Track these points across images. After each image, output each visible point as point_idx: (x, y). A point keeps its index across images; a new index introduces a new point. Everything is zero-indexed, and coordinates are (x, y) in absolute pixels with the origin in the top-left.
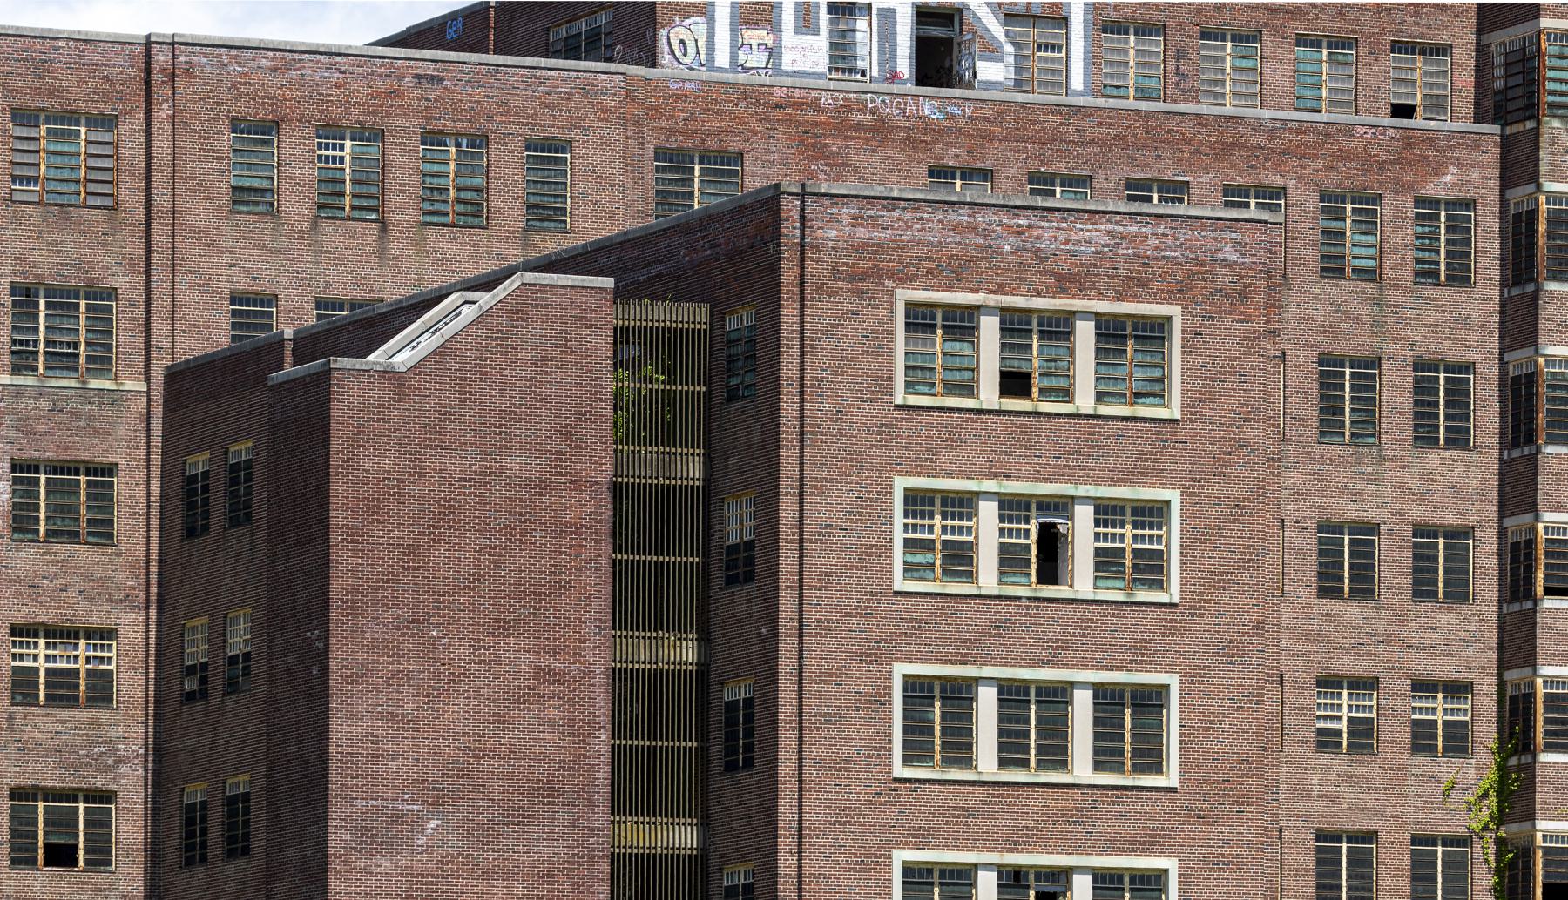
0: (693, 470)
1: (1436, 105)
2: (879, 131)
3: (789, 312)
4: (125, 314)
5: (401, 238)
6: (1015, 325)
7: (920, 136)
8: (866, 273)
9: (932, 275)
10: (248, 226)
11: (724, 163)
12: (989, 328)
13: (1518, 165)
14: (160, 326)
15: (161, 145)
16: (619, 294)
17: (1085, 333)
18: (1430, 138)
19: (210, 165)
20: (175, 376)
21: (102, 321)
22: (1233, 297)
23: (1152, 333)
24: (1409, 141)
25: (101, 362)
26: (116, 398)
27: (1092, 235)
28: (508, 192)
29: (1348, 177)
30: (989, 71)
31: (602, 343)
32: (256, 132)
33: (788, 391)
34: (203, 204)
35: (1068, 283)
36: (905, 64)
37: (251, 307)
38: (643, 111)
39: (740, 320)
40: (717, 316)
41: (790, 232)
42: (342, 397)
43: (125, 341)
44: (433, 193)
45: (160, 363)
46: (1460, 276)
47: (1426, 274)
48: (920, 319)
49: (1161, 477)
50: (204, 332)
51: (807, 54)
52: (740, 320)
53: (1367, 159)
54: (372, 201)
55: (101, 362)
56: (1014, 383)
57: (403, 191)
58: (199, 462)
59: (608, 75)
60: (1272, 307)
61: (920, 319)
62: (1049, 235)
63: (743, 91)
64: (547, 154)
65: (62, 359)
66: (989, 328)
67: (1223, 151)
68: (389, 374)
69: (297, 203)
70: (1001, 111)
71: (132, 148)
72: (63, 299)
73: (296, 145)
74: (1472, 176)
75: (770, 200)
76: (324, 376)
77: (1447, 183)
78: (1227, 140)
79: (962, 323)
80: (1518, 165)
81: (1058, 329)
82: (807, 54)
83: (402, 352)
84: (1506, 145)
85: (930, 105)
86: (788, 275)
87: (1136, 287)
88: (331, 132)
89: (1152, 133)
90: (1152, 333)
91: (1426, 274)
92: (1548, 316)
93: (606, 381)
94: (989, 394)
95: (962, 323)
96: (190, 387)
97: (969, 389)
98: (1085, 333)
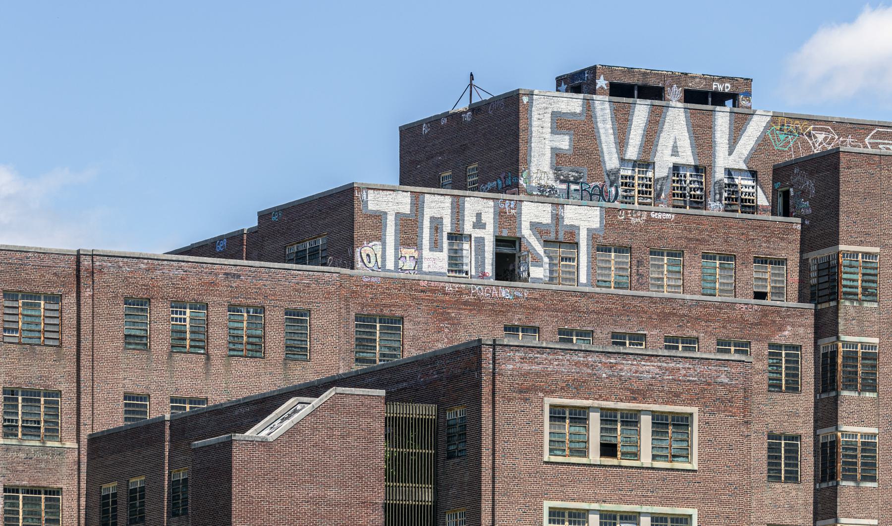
0: (427, 496)
1: (778, 292)
2: (477, 305)
3: (486, 410)
4: (66, 406)
5: (217, 363)
6: (609, 418)
7: (499, 308)
8: (528, 389)
9: (564, 390)
10: (134, 357)
11: (393, 324)
12: (595, 419)
13: (826, 326)
14: (86, 413)
15: (86, 311)
16: (388, 399)
17: (646, 422)
18: (777, 311)
19: (111, 324)
20: (94, 440)
21: (53, 410)
22: (724, 404)
23: (682, 422)
24: (765, 312)
25: (53, 432)
26: (61, 452)
27: (650, 368)
28: (276, 341)
29: (733, 332)
30: (538, 273)
31: (379, 426)
32: (138, 304)
33: (486, 453)
34: (109, 344)
35: (637, 395)
36: (489, 269)
37: (135, 402)
38: (351, 292)
39: (455, 414)
40: (441, 411)
41: (487, 366)
42: (238, 456)
43: (66, 420)
44: (234, 338)
45: (85, 433)
46: (793, 387)
47: (774, 386)
48: (557, 414)
49: (687, 502)
50: (110, 417)
51: (436, 262)
52: (455, 414)
53: (743, 321)
54: (201, 344)
55: (53, 432)
56: (608, 449)
57: (218, 337)
58: (110, 488)
59: (332, 272)
60: (746, 409)
61: (557, 414)
62: (627, 368)
63: (403, 283)
64: (297, 318)
65: (31, 430)
66: (595, 419)
67: (664, 317)
68: (264, 443)
69: (160, 343)
70: (543, 295)
71: (70, 313)
72: (31, 397)
73: (160, 312)
74: (799, 332)
75: (475, 348)
76: (229, 443)
77: (785, 336)
78: (666, 312)
79: (579, 416)
80: (826, 326)
81: (631, 420)
82: (436, 262)
83: (269, 429)
84: (818, 315)
85: (504, 291)
86: (486, 390)
87: (674, 397)
88: (178, 305)
89: (626, 307)
90: (682, 422)
91: (774, 386)
92: (843, 410)
93: (381, 447)
94: (594, 457)
95: (579, 416)
96: (102, 447)
97: (584, 453)
98: (646, 422)
